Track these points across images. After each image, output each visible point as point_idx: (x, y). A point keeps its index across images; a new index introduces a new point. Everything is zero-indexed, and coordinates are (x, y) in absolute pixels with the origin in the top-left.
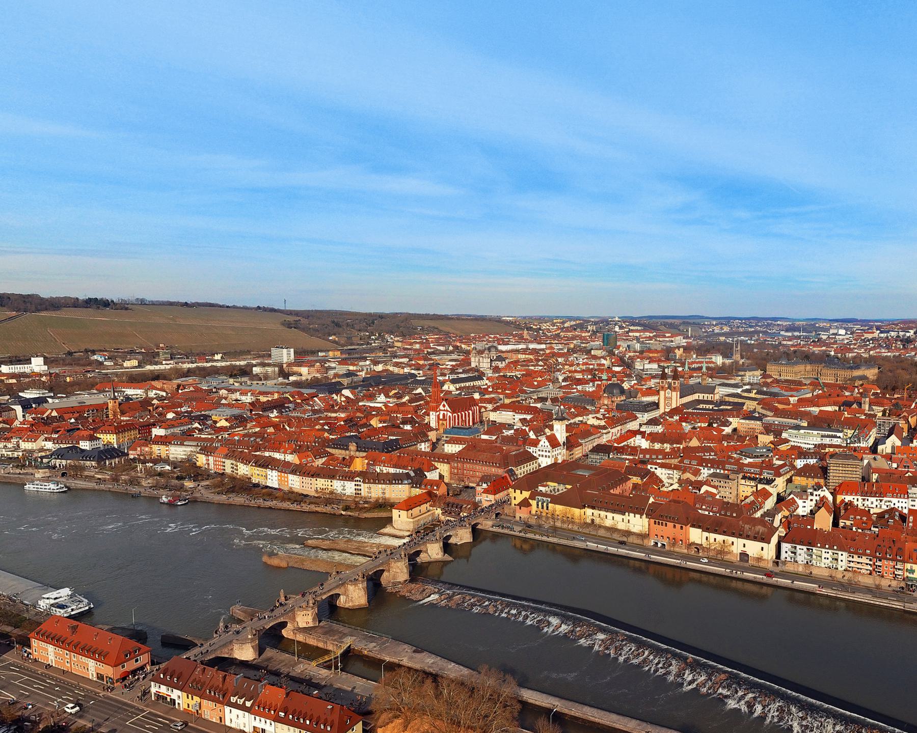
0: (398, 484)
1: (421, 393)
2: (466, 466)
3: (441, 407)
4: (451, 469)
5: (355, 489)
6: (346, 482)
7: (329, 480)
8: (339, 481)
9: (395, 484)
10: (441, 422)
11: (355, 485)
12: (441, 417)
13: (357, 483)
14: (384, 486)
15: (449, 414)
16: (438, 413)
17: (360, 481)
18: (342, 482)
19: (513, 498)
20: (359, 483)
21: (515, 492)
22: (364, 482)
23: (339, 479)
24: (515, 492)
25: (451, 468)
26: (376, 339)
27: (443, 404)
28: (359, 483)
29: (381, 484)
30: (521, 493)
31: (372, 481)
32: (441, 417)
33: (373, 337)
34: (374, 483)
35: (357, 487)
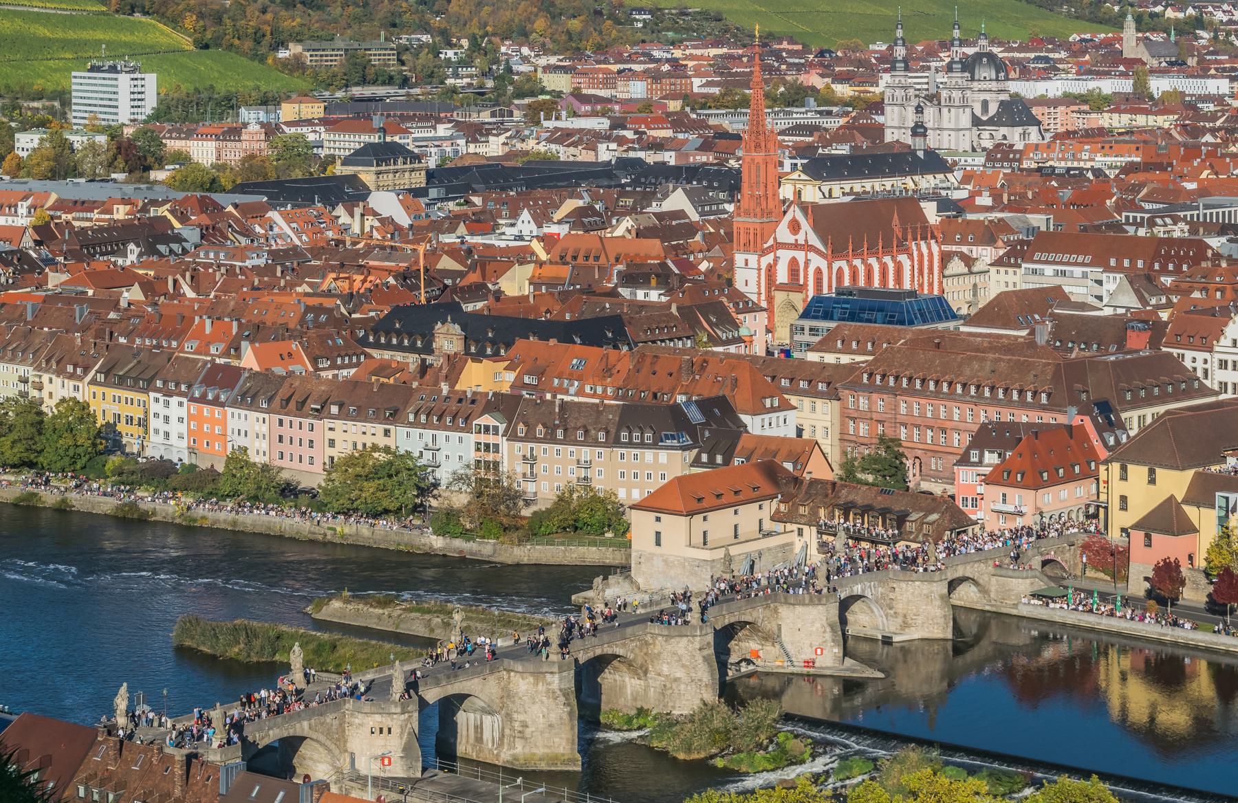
0: (642, 445)
1: (681, 214)
2: (910, 408)
3: (783, 233)
4: (843, 425)
6: (441, 435)
7: (380, 428)
8: (415, 432)
9: (630, 444)
10: (780, 297)
12: (782, 276)
13: (483, 438)
14: (586, 453)
15: (817, 262)
16: (769, 259)
17: (496, 429)
18: (428, 433)
19: (1115, 503)
20: (491, 439)
21: (1124, 477)
22: (512, 436)
23: (416, 424)
24: (1124, 477)
25: (847, 416)
26: (463, 63)
27: (789, 217)
28: (491, 439)
29: (576, 443)
30: (1152, 481)
31: (540, 430)
32: (782, 276)
33: (450, 53)
34: (550, 438)
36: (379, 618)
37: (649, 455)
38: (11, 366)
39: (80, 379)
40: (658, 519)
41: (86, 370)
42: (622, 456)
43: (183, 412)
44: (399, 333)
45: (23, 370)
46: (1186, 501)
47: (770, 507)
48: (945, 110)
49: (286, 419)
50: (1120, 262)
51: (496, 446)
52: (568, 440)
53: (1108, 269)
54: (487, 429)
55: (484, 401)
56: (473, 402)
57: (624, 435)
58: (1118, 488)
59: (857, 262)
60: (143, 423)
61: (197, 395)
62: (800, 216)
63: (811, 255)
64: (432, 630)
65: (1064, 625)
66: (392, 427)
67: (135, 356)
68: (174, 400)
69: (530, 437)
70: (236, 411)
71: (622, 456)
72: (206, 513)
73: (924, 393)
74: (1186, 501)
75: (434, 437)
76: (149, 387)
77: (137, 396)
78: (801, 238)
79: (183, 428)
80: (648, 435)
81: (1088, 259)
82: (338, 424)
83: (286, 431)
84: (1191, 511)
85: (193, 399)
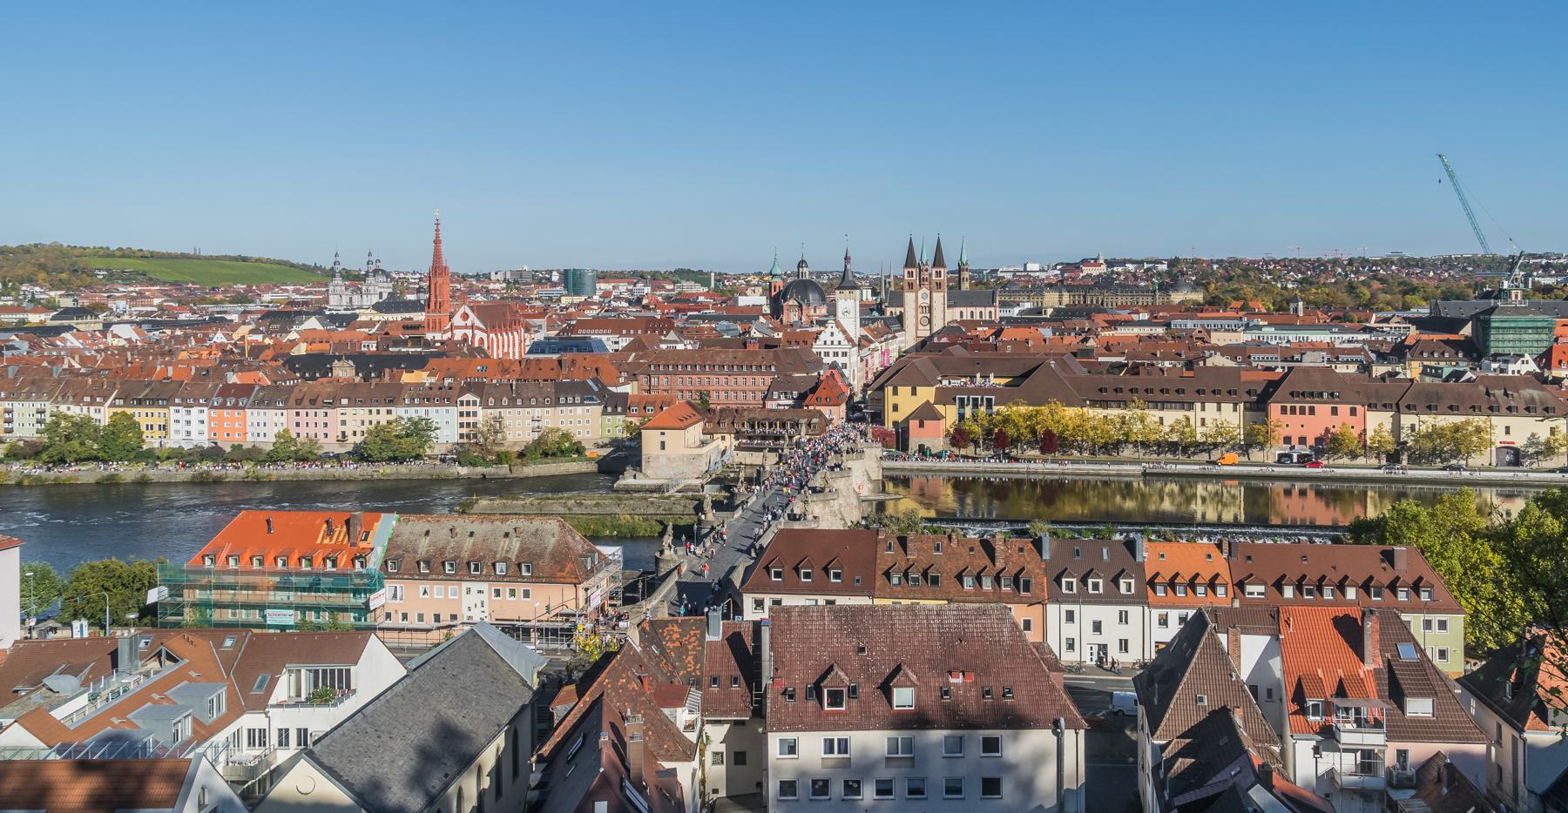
0: (574, 404)
3: (457, 320)
5: (461, 425)
6: (432, 410)
7: (383, 410)
9: (566, 404)
11: (461, 414)
13: (465, 409)
14: (538, 412)
20: (471, 409)
22: (485, 406)
24: (895, 393)
27: (461, 311)
28: (471, 409)
30: (914, 393)
31: (505, 401)
34: (512, 404)
35: (465, 420)
36: (524, 506)
37: (579, 410)
38: (26, 404)
39: (101, 404)
40: (663, 434)
41: (105, 401)
42: (562, 412)
43: (205, 417)
44: (299, 370)
45: (38, 405)
46: (936, 403)
47: (699, 427)
48: (364, 296)
49: (303, 412)
50: (636, 332)
51: (475, 414)
52: (526, 404)
53: (622, 335)
54: (468, 403)
55: (458, 388)
56: (450, 388)
57: (562, 400)
58: (890, 399)
59: (492, 335)
60: (164, 427)
61: (216, 404)
62: (468, 311)
63: (476, 331)
64: (569, 509)
65: (911, 470)
66: (393, 409)
67: (146, 386)
68: (195, 410)
69: (498, 405)
70: (255, 411)
71: (562, 412)
72: (271, 472)
73: (685, 372)
74: (936, 403)
75: (427, 412)
76: (169, 402)
77: (156, 411)
78: (469, 323)
79: (205, 427)
80: (578, 399)
81: (609, 331)
82: (350, 411)
83: (302, 419)
84: (941, 408)
85: (213, 407)
